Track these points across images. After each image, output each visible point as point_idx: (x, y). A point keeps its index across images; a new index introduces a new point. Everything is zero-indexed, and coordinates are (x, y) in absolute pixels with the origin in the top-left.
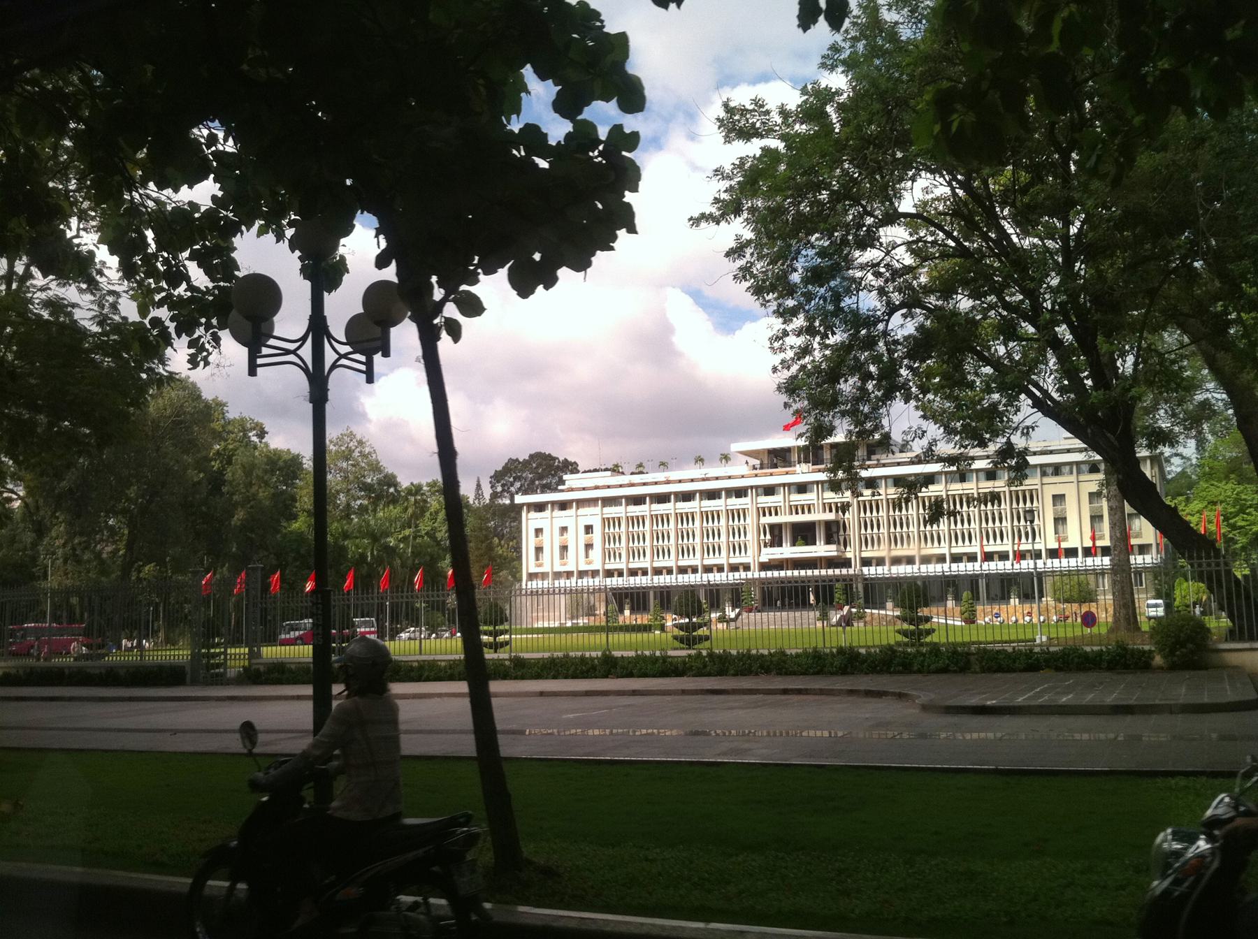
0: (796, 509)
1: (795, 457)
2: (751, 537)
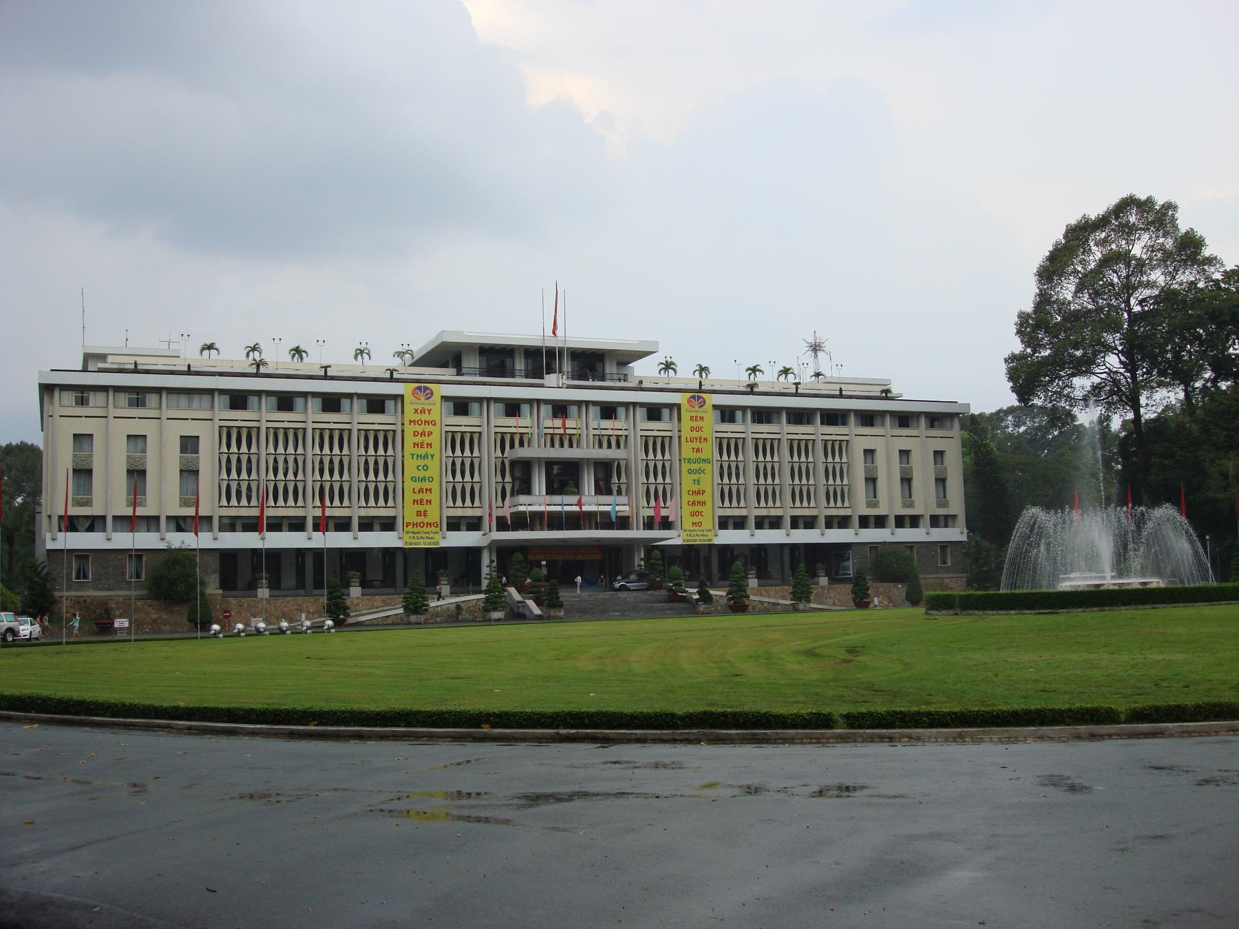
1: (520, 365)
2: (489, 481)
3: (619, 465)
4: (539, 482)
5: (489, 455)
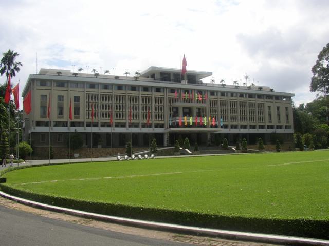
0: (184, 101)
2: (166, 112)
3: (203, 109)
4: (181, 112)
5: (166, 104)
